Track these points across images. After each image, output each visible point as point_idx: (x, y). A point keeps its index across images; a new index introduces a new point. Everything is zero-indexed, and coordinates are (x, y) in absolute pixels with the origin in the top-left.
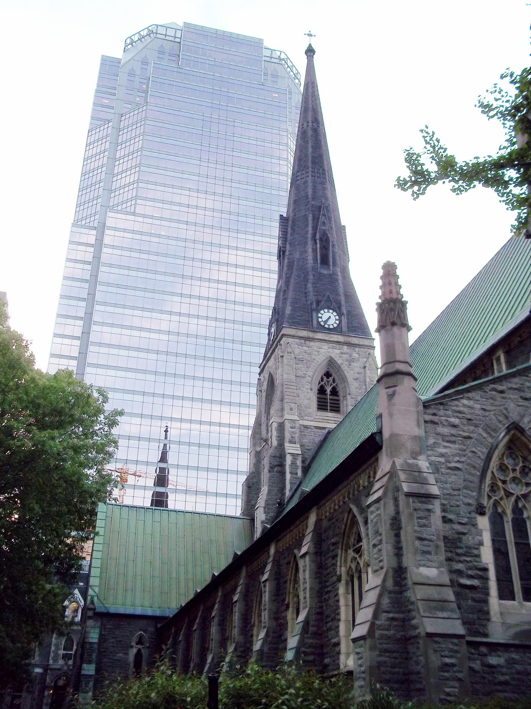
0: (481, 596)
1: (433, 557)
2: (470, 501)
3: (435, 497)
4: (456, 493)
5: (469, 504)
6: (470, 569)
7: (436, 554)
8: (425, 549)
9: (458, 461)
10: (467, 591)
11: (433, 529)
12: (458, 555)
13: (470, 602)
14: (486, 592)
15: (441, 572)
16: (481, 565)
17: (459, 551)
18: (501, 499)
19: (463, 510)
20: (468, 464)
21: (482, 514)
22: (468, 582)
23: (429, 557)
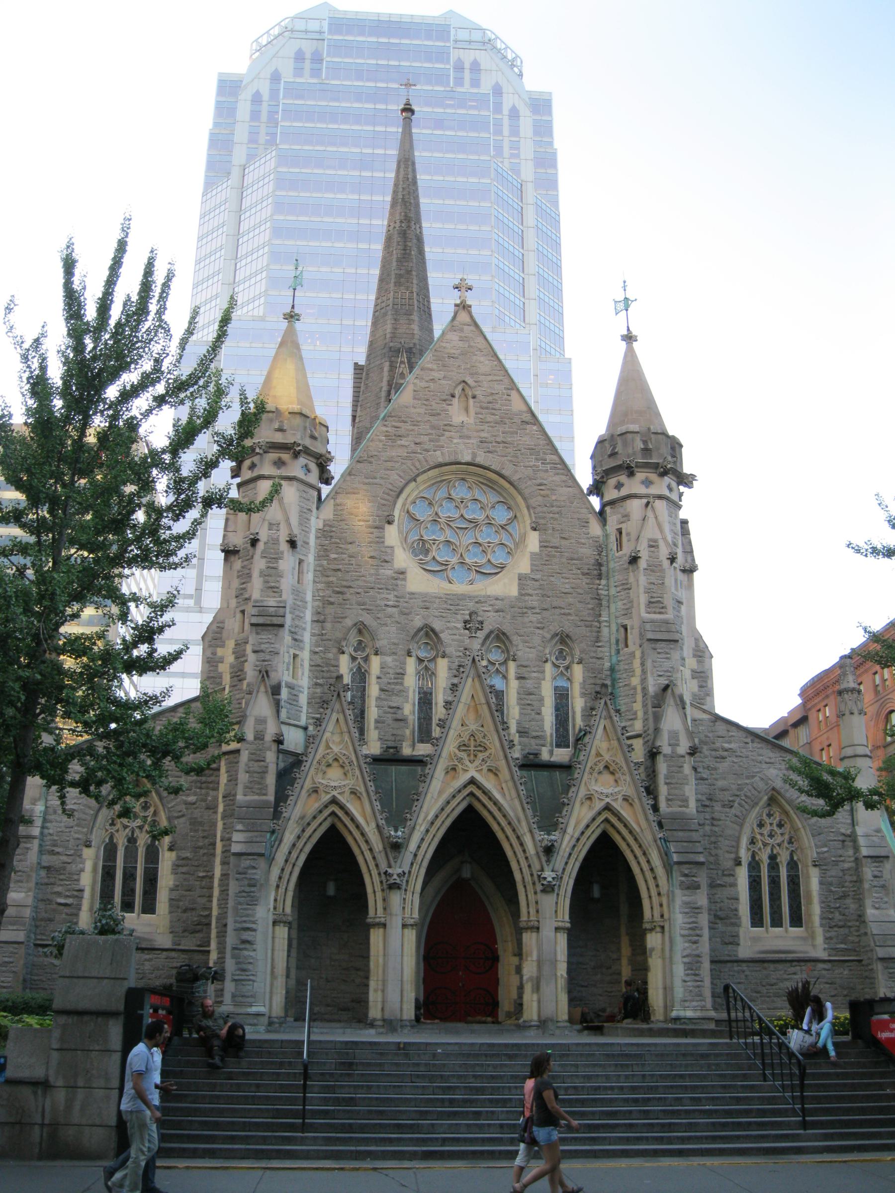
0: (74, 911)
1: (25, 885)
2: (80, 836)
3: (34, 837)
4: (68, 830)
5: (78, 839)
6: (68, 890)
7: (27, 881)
8: (19, 878)
9: (75, 803)
10: (62, 908)
11: (28, 863)
12: (62, 880)
13: (64, 916)
14: (79, 908)
15: (28, 896)
16: (77, 888)
17: (62, 877)
18: (117, 831)
19: (72, 843)
20: (85, 805)
21: (88, 845)
22: (62, 901)
23: (20, 884)
